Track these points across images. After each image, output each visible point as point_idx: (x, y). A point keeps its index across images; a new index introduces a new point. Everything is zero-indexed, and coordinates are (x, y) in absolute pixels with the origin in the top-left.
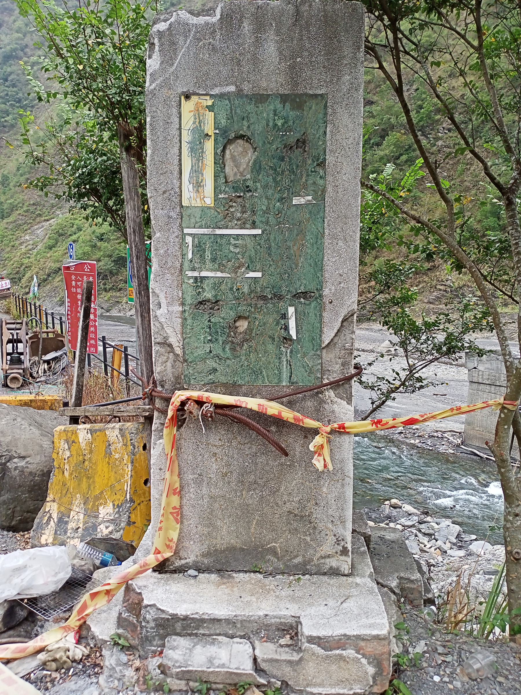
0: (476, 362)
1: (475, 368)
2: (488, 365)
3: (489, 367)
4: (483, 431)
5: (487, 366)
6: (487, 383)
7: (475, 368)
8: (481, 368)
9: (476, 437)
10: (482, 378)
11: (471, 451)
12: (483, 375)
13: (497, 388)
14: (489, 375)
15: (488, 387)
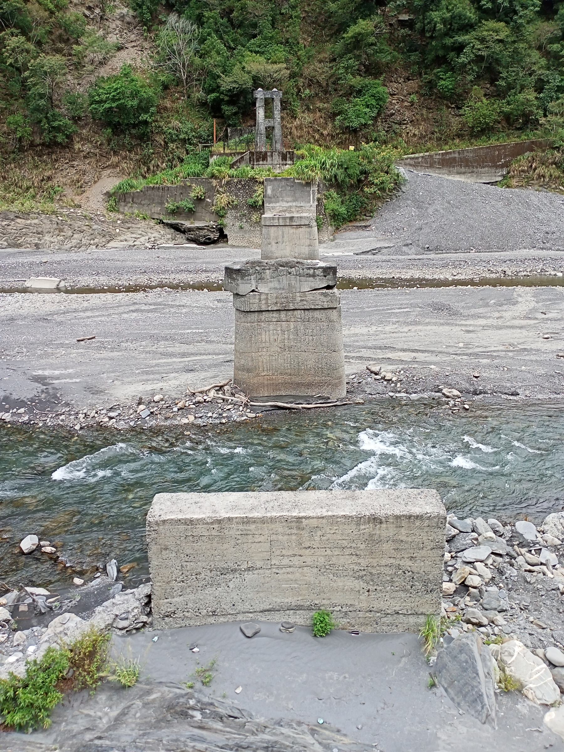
0: (253, 282)
1: (253, 291)
2: (275, 284)
3: (277, 286)
4: (273, 374)
5: (272, 285)
6: (275, 308)
7: (253, 291)
8: (263, 288)
9: (263, 385)
10: (267, 303)
11: (271, 406)
12: (267, 299)
13: (290, 313)
14: (277, 298)
15: (275, 315)
